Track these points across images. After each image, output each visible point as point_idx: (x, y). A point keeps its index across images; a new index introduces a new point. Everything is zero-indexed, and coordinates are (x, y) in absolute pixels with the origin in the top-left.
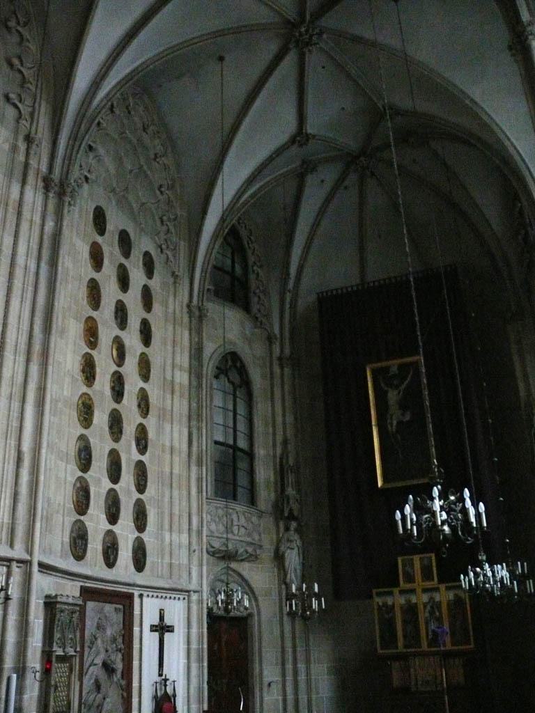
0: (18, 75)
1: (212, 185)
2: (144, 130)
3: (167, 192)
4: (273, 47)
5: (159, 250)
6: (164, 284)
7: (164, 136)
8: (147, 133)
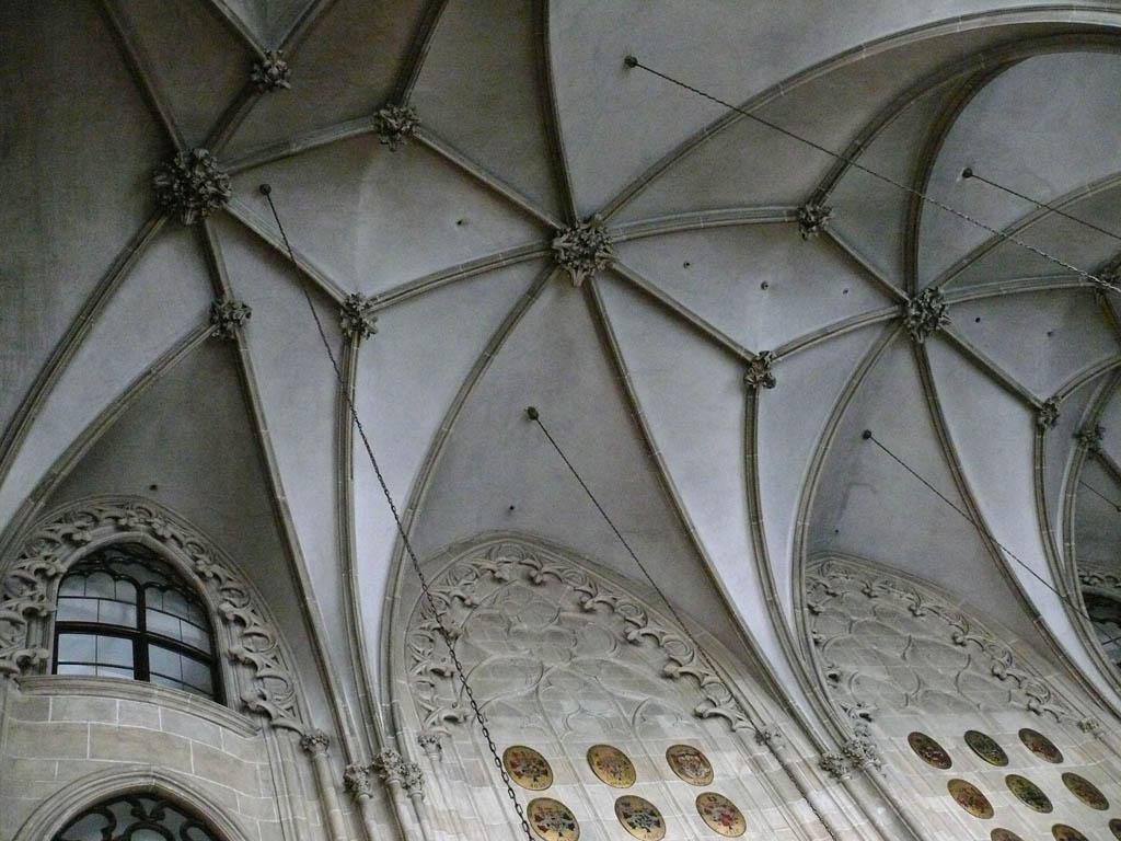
0: (687, 681)
1: (1006, 573)
2: (869, 596)
3: (967, 637)
4: (904, 363)
5: (1033, 713)
6: (1084, 751)
7: (898, 579)
8: (876, 596)
